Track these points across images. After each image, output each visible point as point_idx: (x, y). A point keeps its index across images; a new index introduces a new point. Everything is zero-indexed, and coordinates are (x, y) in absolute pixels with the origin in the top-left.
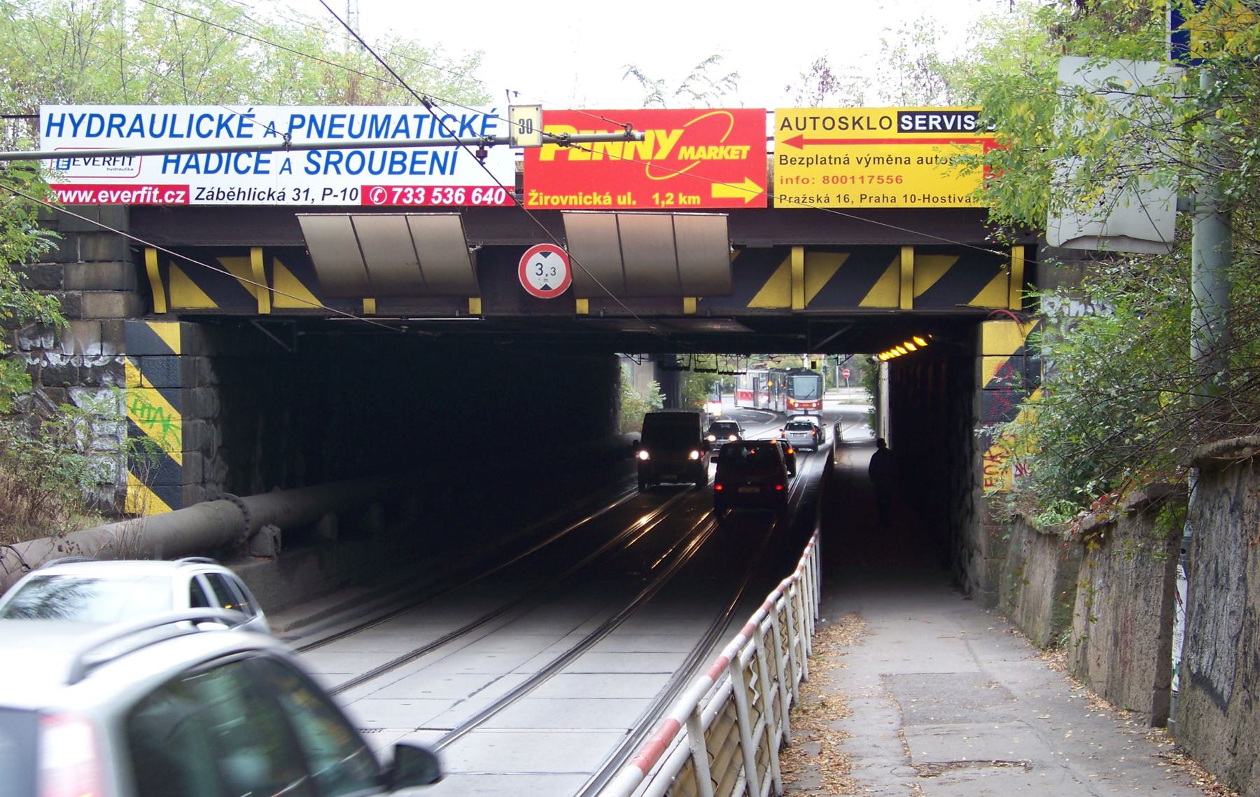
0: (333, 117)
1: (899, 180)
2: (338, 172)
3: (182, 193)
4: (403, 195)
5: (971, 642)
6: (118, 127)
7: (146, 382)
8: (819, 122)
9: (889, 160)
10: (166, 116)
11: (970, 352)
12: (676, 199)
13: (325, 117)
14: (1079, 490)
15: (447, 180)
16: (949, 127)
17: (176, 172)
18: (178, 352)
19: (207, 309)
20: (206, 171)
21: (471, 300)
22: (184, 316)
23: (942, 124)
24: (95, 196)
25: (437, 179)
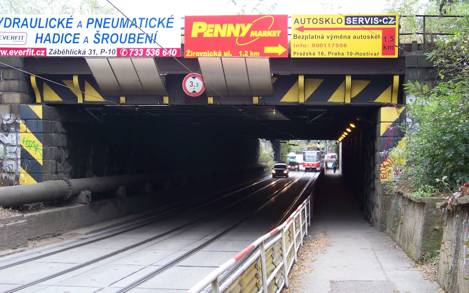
0: (105, 19)
1: (345, 45)
2: (107, 43)
3: (43, 51)
4: (134, 52)
5: (377, 252)
6: (17, 23)
7: (28, 130)
8: (311, 21)
9: (341, 37)
10: (37, 19)
12: (249, 54)
13: (102, 19)
14: (438, 180)
15: (153, 45)
16: (367, 22)
17: (41, 42)
18: (41, 118)
19: (58, 101)
20: (53, 42)
21: (164, 98)
23: (364, 21)
24: (8, 52)
25: (148, 45)
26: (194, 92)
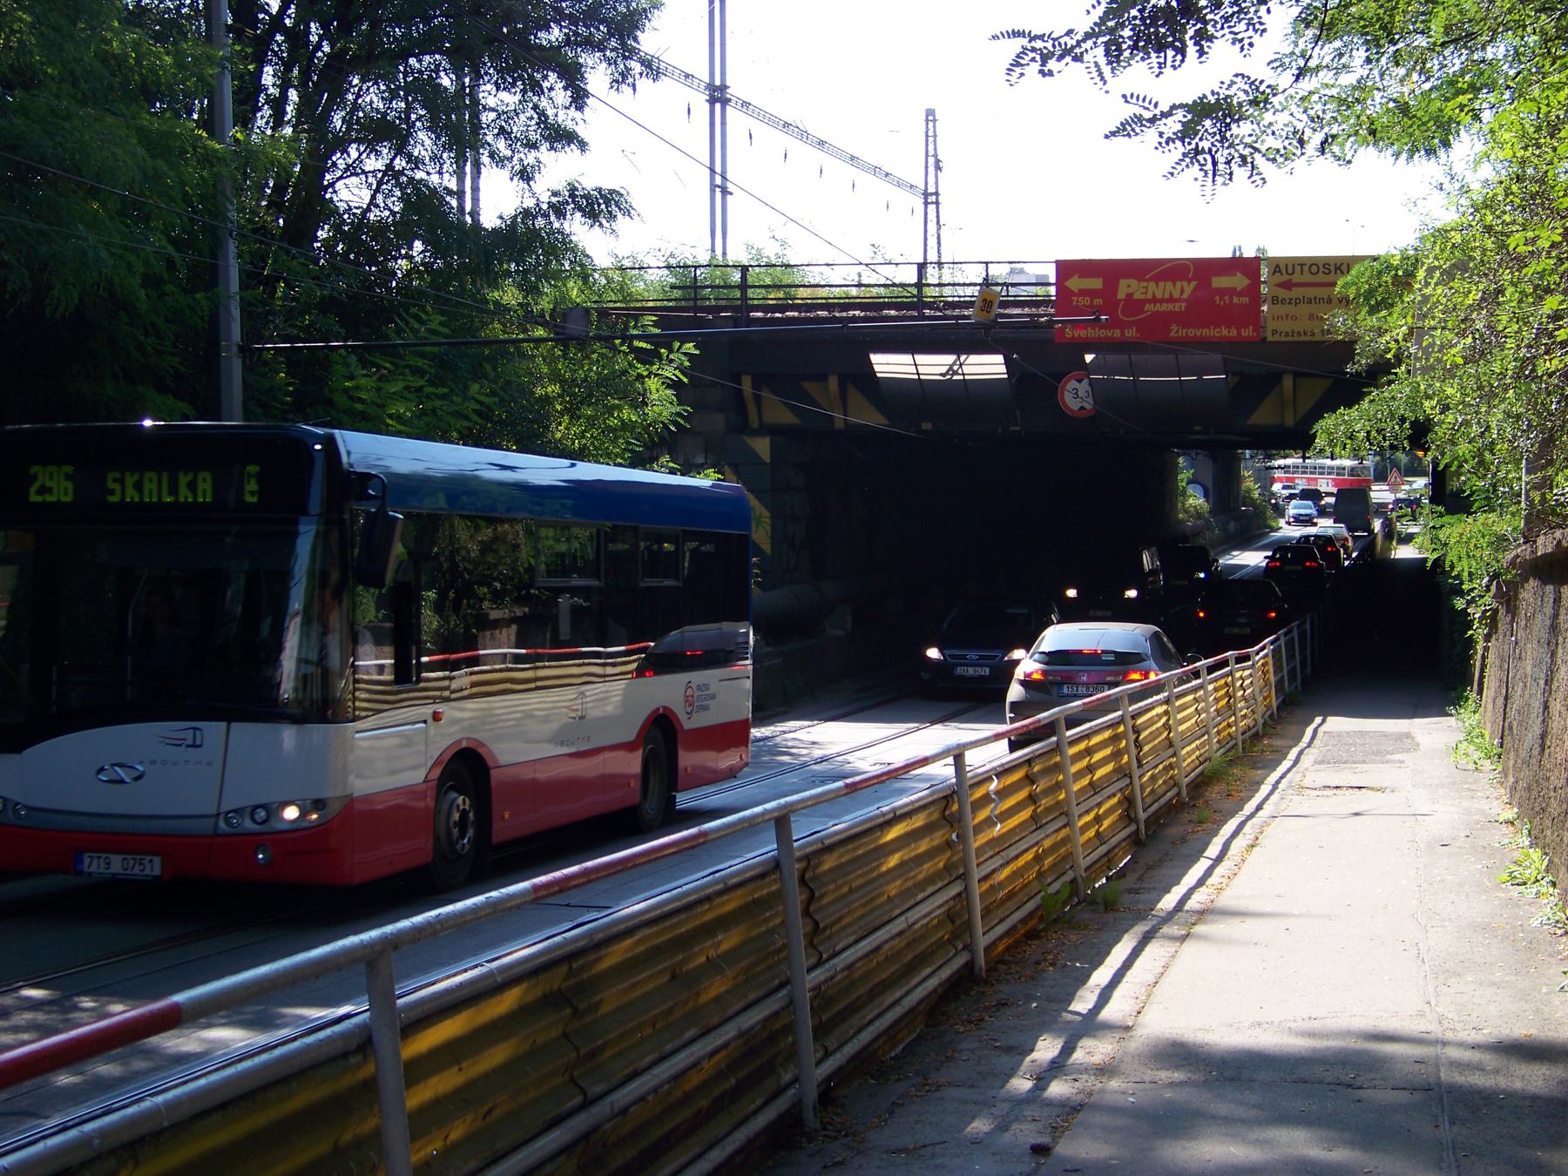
22: (774, 431)
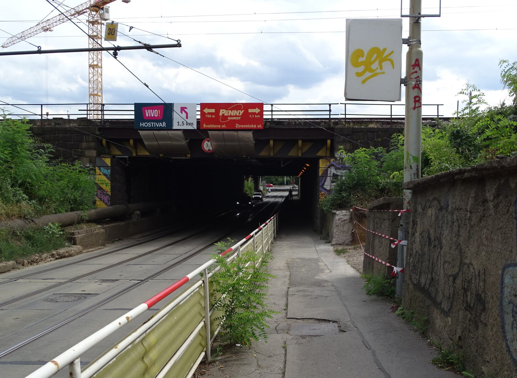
11: (317, 167)
26: (209, 150)
